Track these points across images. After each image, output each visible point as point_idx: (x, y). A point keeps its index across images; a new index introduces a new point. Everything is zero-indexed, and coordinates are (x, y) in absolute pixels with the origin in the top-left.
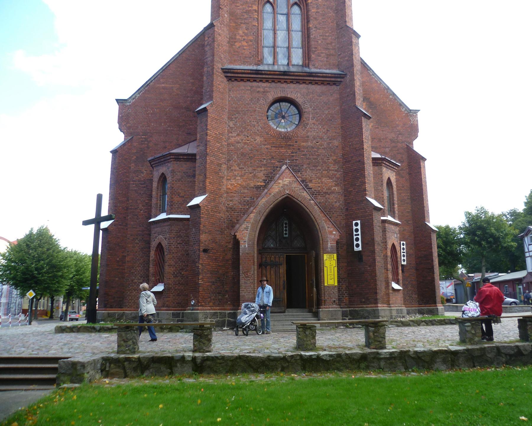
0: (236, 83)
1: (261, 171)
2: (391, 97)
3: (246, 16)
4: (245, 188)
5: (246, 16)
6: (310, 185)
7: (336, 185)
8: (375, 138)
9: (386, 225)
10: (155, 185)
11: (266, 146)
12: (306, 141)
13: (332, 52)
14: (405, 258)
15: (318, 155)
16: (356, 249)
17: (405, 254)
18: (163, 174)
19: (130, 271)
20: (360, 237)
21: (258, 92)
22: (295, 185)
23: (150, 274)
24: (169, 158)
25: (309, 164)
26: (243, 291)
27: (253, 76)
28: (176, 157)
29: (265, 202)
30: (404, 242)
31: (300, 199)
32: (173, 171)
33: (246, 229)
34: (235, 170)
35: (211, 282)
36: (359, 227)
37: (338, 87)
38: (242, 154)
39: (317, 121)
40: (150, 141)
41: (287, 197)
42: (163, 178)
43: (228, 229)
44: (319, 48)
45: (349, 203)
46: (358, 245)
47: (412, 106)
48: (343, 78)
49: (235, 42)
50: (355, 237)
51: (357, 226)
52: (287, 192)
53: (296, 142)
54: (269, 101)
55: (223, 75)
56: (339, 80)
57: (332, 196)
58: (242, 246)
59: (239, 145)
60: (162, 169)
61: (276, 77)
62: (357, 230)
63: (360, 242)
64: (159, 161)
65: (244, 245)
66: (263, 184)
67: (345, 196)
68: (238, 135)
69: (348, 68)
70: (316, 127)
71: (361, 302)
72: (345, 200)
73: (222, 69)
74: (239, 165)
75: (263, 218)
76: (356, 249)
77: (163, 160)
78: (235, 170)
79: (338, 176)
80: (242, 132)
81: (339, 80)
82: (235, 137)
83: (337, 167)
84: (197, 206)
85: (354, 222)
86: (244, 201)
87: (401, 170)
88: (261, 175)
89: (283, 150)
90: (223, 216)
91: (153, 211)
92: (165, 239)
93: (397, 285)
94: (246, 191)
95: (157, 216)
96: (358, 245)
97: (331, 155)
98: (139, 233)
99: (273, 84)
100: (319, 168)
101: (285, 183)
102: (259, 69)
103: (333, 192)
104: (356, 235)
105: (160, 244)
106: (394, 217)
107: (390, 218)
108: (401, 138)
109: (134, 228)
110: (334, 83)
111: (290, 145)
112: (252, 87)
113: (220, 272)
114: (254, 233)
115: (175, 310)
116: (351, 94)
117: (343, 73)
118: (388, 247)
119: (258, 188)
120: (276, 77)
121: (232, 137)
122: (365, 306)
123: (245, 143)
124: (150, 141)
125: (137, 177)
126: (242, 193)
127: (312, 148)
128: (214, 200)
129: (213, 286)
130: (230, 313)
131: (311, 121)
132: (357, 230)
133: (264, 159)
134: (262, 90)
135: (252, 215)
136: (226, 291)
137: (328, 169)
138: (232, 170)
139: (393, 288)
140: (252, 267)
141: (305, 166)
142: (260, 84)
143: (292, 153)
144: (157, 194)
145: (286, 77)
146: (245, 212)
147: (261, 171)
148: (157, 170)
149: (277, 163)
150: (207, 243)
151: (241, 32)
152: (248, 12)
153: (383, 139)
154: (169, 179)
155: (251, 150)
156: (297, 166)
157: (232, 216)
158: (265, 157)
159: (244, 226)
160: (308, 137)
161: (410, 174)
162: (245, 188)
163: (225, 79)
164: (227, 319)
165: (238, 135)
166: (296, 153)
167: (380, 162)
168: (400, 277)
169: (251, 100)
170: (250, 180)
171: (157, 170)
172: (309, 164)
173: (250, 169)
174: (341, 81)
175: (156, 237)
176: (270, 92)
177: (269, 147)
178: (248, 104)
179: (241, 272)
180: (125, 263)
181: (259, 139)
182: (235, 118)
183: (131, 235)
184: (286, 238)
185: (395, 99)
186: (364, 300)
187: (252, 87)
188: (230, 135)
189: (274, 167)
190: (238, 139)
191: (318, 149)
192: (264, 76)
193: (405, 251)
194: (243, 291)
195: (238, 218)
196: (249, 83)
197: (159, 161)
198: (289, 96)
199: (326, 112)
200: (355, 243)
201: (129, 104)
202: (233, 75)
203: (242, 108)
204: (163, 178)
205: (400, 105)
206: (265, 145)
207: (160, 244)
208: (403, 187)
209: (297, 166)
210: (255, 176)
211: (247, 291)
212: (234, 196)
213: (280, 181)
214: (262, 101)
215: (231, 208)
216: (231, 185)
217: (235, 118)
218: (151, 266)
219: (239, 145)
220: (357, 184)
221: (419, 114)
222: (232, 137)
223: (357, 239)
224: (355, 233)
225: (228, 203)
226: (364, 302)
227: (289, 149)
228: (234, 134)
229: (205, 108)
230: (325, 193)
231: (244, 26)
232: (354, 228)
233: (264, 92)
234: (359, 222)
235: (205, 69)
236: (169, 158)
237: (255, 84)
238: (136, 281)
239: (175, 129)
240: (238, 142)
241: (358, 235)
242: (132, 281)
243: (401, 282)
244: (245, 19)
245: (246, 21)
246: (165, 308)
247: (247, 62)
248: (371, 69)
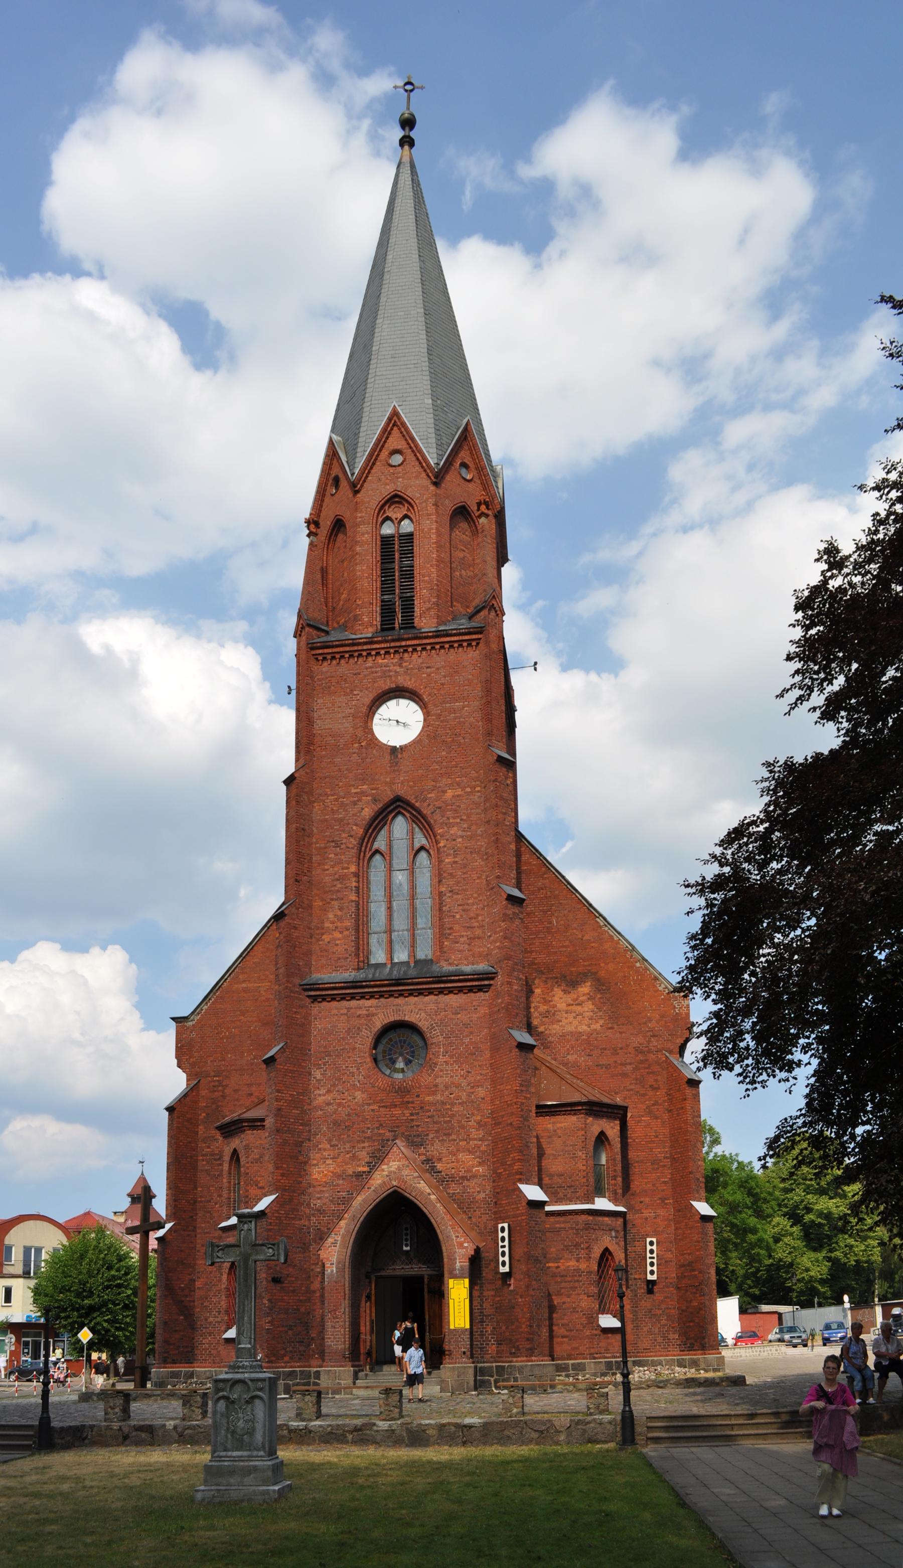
3: (339, 886)
4: (339, 1177)
5: (339, 886)
6: (439, 1166)
7: (480, 1164)
11: (371, 1107)
12: (434, 1093)
13: (478, 932)
15: (453, 1116)
25: (437, 1131)
38: (335, 1123)
39: (451, 1056)
44: (456, 927)
49: (322, 934)
53: (418, 1096)
57: (473, 1183)
59: (330, 1109)
66: (366, 1169)
70: (449, 1068)
74: (330, 1141)
79: (483, 1148)
80: (334, 1085)
83: (481, 1133)
88: (364, 1155)
89: (397, 1112)
97: (473, 1114)
100: (454, 1137)
103: (474, 1176)
110: (480, 989)
111: (408, 1102)
119: (359, 1175)
123: (339, 1105)
127: (443, 1103)
131: (441, 1059)
137: (468, 1139)
141: (431, 1136)
143: (412, 1114)
149: (388, 1134)
151: (331, 916)
152: (342, 878)
155: (349, 1115)
160: (436, 1086)
165: (329, 1091)
169: (349, 1031)
172: (437, 1131)
173: (348, 1146)
177: (375, 1107)
178: (343, 1039)
181: (359, 1095)
187: (349, 1009)
190: (329, 1097)
191: (453, 1104)
199: (467, 1040)
202: (318, 993)
206: (369, 1104)
209: (419, 1136)
214: (365, 1032)
227: (407, 1108)
230: (464, 1178)
231: (336, 904)
233: (368, 1016)
237: (354, 1003)
240: (329, 1104)
244: (338, 891)
245: (340, 895)
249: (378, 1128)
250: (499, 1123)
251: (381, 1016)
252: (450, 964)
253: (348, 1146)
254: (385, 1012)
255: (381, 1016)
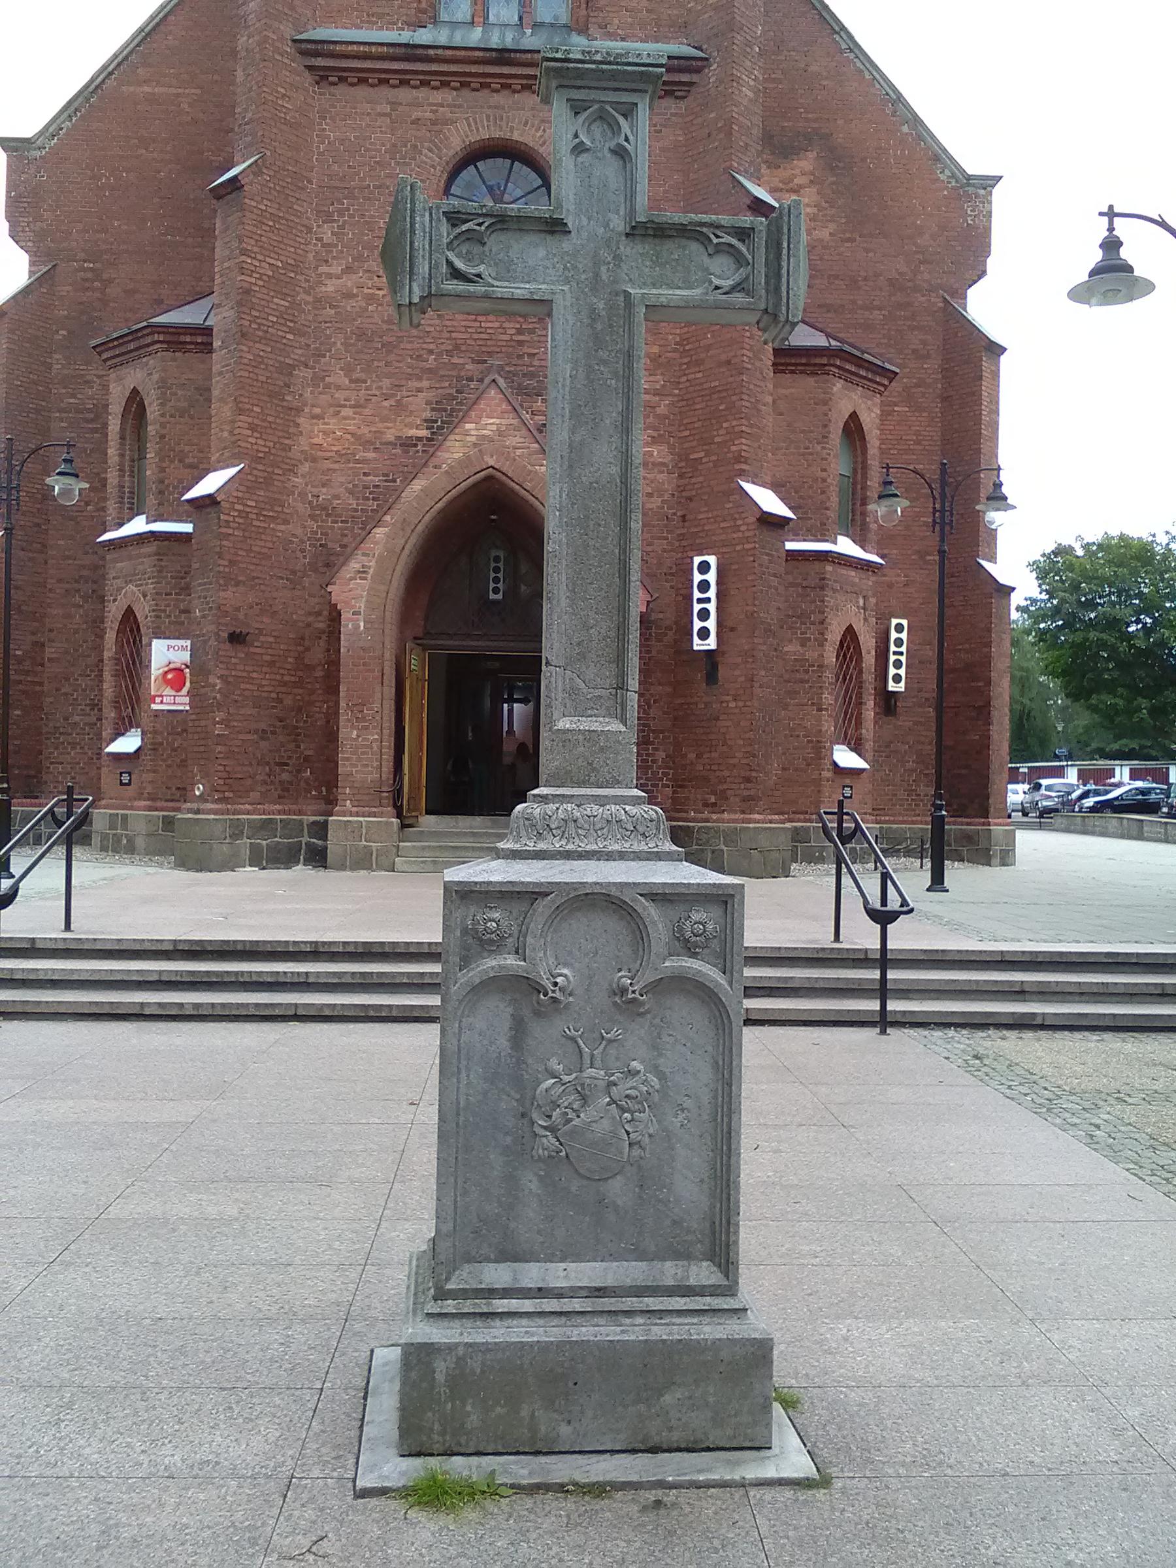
0: (342, 90)
1: (419, 390)
2: (905, 129)
8: (837, 277)
9: (829, 568)
10: (114, 426)
14: (902, 672)
16: (698, 644)
17: (903, 659)
18: (135, 392)
19: (57, 690)
20: (712, 607)
21: (416, 122)
22: (515, 440)
23: (105, 702)
24: (149, 340)
26: (348, 759)
27: (396, 66)
28: (169, 338)
29: (424, 495)
30: (905, 622)
31: (528, 485)
32: (163, 385)
33: (362, 572)
34: (338, 388)
35: (256, 732)
36: (711, 577)
37: (682, 104)
38: (361, 334)
40: (110, 281)
41: (490, 478)
42: (135, 405)
43: (316, 571)
45: (690, 499)
46: (704, 634)
47: (973, 167)
48: (698, 71)
50: (697, 607)
51: (706, 570)
52: (491, 462)
54: (452, 153)
55: (298, 64)
56: (685, 78)
58: (347, 626)
59: (350, 305)
60: (134, 376)
61: (474, 69)
62: (704, 587)
63: (711, 624)
64: (123, 349)
65: (354, 625)
66: (424, 433)
67: (681, 476)
68: (348, 270)
69: (716, 35)
71: (706, 805)
72: (681, 489)
73: (294, 41)
74: (348, 370)
75: (413, 540)
76: (698, 644)
77: (132, 346)
78: (338, 388)
79: (662, 410)
80: (359, 258)
81: (685, 78)
82: (338, 277)
84: (209, 500)
85: (697, 560)
86: (365, 487)
87: (917, 386)
88: (420, 405)
89: (491, 323)
90: (299, 532)
91: (112, 507)
92: (145, 596)
93: (854, 755)
94: (371, 455)
95: (121, 525)
96: (704, 634)
98: (85, 573)
99: (466, 92)
101: (488, 435)
102: (418, 41)
104: (700, 601)
105: (129, 612)
106: (861, 542)
107: (845, 546)
108: (926, 276)
109: (68, 558)
112: (395, 104)
113: (288, 701)
114: (383, 588)
115: (228, 812)
116: (719, 130)
117: (702, 55)
118: (829, 637)
119: (408, 444)
120: (474, 69)
121: (330, 276)
122: (714, 817)
124: (110, 281)
125: (73, 396)
126: (358, 462)
128: (268, 481)
129: (263, 744)
130: (314, 823)
132: (704, 587)
133: (431, 352)
134: (428, 115)
135: (380, 532)
136: (307, 759)
138: (328, 386)
139: (835, 764)
140: (378, 688)
142: (422, 93)
143: (520, 331)
144: (122, 455)
145: (506, 70)
146: (373, 520)
147: (419, 390)
148: (120, 379)
150: (241, 616)
153: (865, 279)
154: (153, 411)
156: (532, 376)
157: (326, 534)
158: (432, 346)
159: (354, 565)
161: (945, 399)
162: (367, 444)
163: (308, 78)
164: (305, 839)
165: (348, 270)
166: (532, 331)
167: (824, 361)
168: (868, 730)
169: (393, 150)
170: (384, 419)
171: (120, 379)
173: (386, 382)
174: (691, 84)
175: (119, 589)
176: (453, 122)
179: (342, 704)
180: (42, 665)
182: (341, 214)
183: (60, 581)
184: (495, 603)
185: (920, 138)
186: (713, 800)
188: (324, 269)
189: (459, 378)
190: (349, 282)
192: (434, 67)
193: (904, 649)
194: (348, 759)
195: (345, 540)
196: (385, 92)
197: (123, 349)
198: (516, 136)
200: (697, 624)
201: (37, 154)
202: (331, 63)
203: (362, 180)
204: (135, 405)
205: (936, 158)
207: (129, 612)
208: (918, 442)
210: (400, 407)
211: (359, 759)
212: (335, 470)
213: (468, 426)
215: (325, 509)
216: (326, 433)
217: (341, 213)
218: (107, 676)
219: (350, 305)
220: (717, 439)
221: (997, 192)
222: (330, 276)
223: (703, 615)
224: (697, 594)
225: (315, 491)
226: (714, 805)
228: (336, 269)
229: (234, 179)
232: (697, 577)
233: (434, 123)
234: (712, 560)
235: (242, 40)
236: (149, 340)
237: (405, 94)
238: (77, 719)
239: (190, 240)
240: (349, 296)
241: (708, 600)
242: (66, 719)
243: (869, 745)
246: (143, 803)
247: (381, 16)
248: (843, 28)
249: (449, 353)
250: (698, 363)
251: (462, 126)
252: (611, 36)
253: (386, 382)
254: (470, 119)
255: (462, 126)
